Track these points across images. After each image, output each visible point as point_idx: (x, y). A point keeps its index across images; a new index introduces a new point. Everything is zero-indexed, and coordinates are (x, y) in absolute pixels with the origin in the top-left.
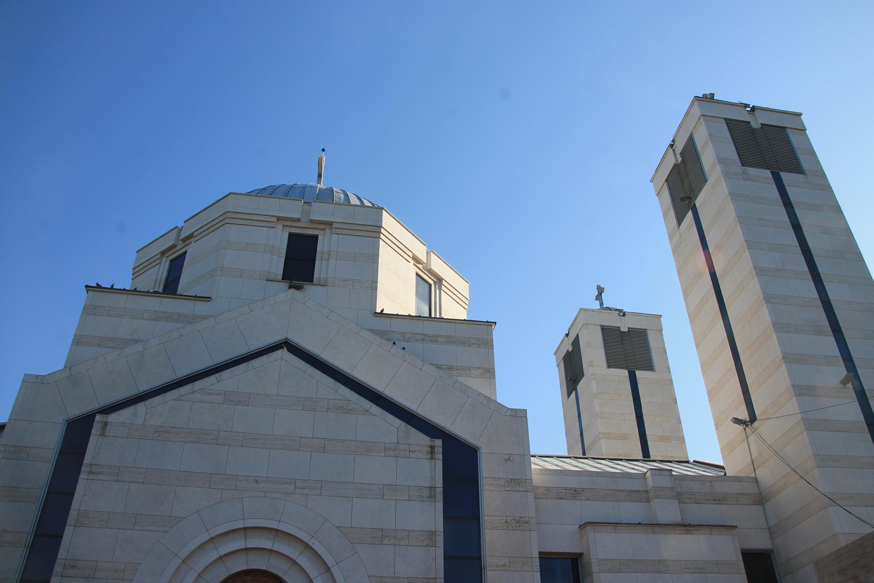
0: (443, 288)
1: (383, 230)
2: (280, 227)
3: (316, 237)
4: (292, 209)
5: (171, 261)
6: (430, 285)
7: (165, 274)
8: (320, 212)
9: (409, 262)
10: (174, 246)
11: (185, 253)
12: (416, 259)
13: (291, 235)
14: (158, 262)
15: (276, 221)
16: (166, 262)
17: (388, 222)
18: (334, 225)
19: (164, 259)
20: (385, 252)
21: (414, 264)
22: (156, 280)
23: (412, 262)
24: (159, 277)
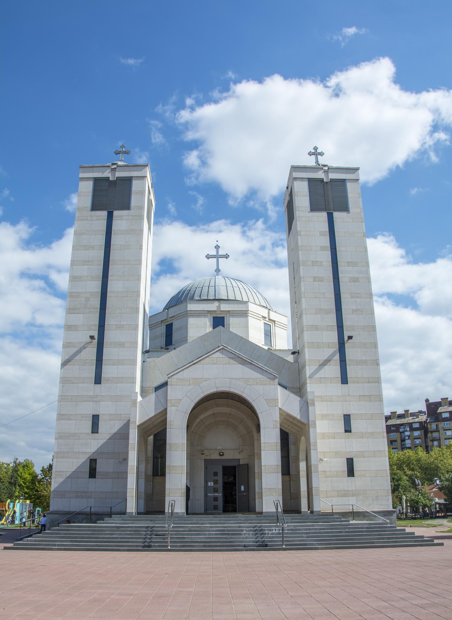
0: (276, 325)
1: (249, 312)
2: (209, 315)
3: (224, 317)
4: (213, 307)
5: (166, 325)
6: (270, 325)
7: (165, 332)
8: (225, 307)
9: (261, 320)
10: (166, 319)
11: (172, 324)
12: (264, 318)
13: (213, 317)
14: (160, 325)
15: (207, 313)
16: (164, 325)
17: (252, 307)
18: (230, 312)
19: (163, 324)
20: (251, 321)
21: (263, 319)
22: (161, 334)
23: (262, 319)
24: (163, 332)
